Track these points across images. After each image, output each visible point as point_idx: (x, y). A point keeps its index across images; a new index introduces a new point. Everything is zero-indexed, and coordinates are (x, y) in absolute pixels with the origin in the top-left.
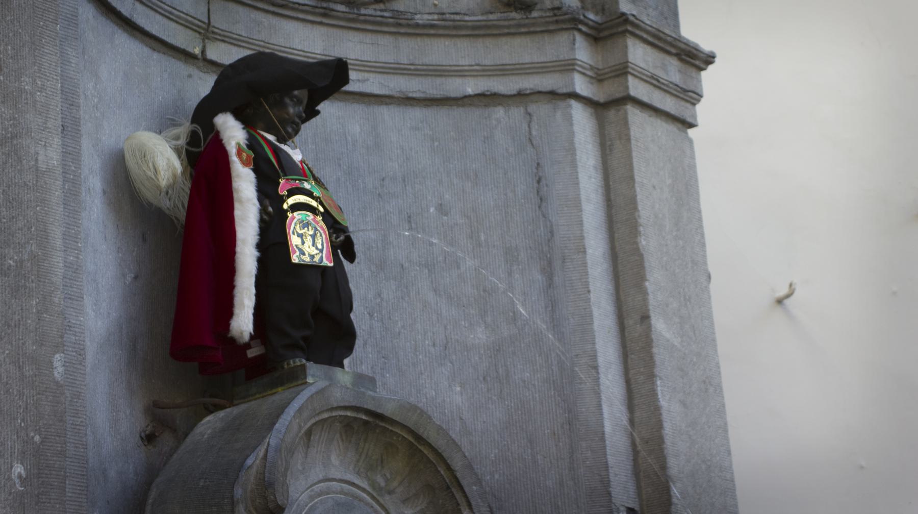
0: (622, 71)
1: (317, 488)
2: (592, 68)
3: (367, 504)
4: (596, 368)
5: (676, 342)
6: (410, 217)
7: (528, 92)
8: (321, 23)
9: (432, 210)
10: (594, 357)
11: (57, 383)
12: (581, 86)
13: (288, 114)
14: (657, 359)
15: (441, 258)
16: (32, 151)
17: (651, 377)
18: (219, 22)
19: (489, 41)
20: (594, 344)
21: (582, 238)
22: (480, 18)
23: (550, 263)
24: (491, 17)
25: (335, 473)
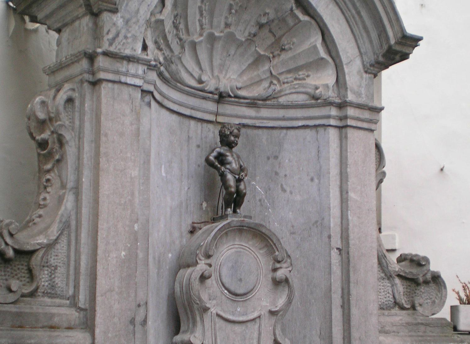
0: (346, 117)
1: (230, 247)
2: (337, 116)
3: (247, 250)
4: (330, 208)
5: (359, 199)
6: (280, 163)
7: (317, 124)
8: (254, 107)
9: (287, 161)
10: (330, 205)
11: (136, 231)
12: (332, 122)
13: (232, 140)
14: (349, 205)
15: (288, 175)
16: (130, 172)
17: (347, 210)
18: (221, 111)
19: (306, 110)
20: (330, 201)
21: (329, 169)
22: (303, 102)
23: (320, 176)
24: (306, 102)
25: (236, 243)
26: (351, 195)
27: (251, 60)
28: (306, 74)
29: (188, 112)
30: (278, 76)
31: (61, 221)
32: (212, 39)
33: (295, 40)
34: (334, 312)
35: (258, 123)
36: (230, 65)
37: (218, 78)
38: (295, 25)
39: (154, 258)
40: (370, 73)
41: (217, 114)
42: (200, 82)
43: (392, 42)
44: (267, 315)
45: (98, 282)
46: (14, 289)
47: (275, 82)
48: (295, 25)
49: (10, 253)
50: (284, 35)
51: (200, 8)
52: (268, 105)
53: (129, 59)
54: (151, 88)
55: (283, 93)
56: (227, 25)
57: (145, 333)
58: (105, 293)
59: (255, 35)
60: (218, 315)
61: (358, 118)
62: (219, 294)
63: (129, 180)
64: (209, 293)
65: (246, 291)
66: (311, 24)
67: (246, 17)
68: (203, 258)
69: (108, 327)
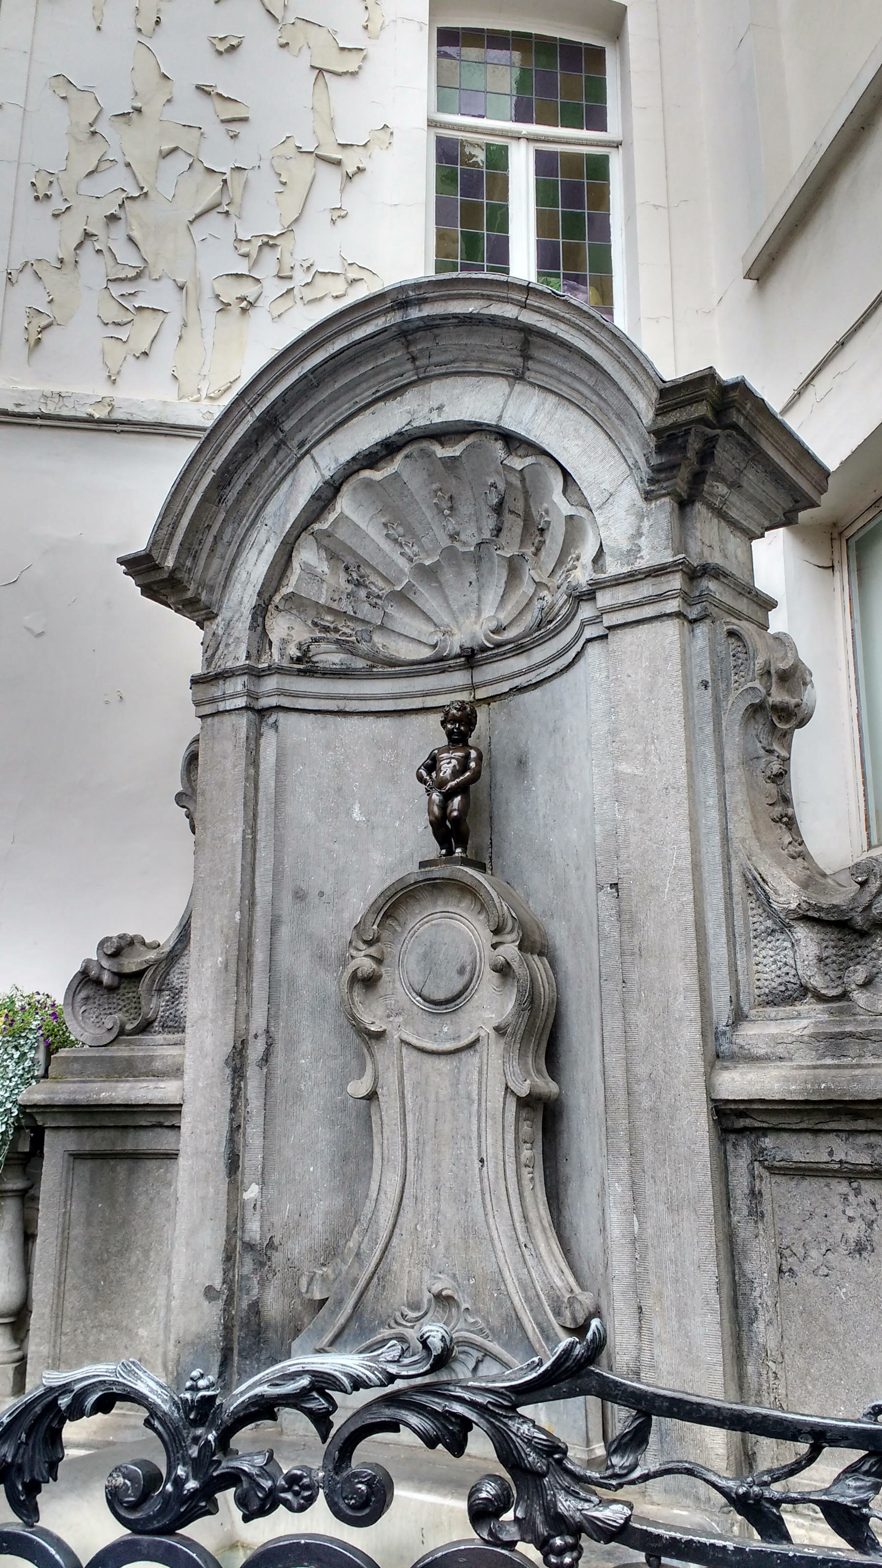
1: (425, 920)
8: (524, 651)
18: (478, 679)
27: (505, 574)
28: (574, 556)
29: (417, 703)
30: (545, 580)
32: (429, 574)
33: (545, 505)
34: (608, 1018)
35: (533, 677)
36: (479, 598)
38: (523, 480)
39: (320, 957)
42: (435, 646)
44: (493, 1034)
47: (546, 592)
48: (523, 480)
50: (527, 506)
51: (387, 536)
52: (537, 640)
54: (273, 701)
55: (557, 608)
56: (454, 537)
58: (196, 1022)
59: (498, 531)
60: (402, 1041)
61: (623, 604)
62: (408, 1005)
63: (229, 849)
64: (386, 1005)
65: (449, 995)
66: (540, 464)
67: (466, 509)
68: (364, 947)
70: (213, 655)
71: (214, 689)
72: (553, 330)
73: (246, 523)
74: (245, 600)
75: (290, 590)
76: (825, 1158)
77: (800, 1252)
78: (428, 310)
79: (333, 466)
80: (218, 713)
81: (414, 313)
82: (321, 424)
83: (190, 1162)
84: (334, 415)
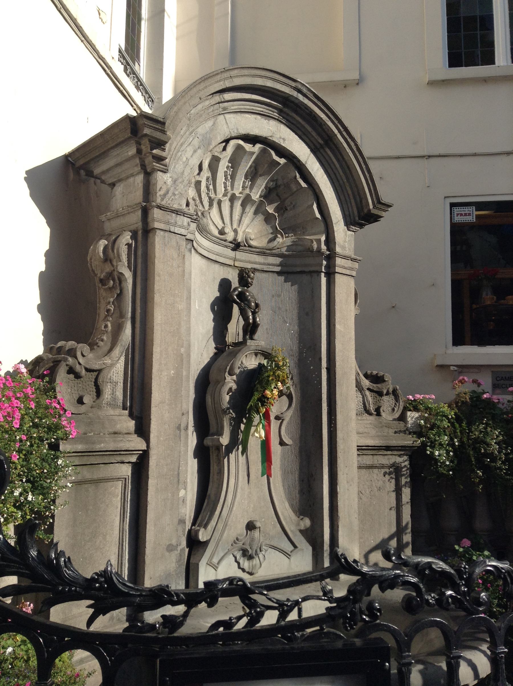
5: (342, 330)
26: (338, 327)
29: (213, 257)
31: (121, 345)
32: (233, 199)
37: (236, 231)
40: (351, 231)
41: (235, 260)
43: (371, 207)
45: (152, 395)
46: (85, 400)
47: (279, 236)
48: (297, 190)
49: (83, 372)
50: (287, 198)
51: (226, 172)
53: (177, 212)
57: (187, 435)
69: (160, 432)
70: (165, 195)
71: (169, 217)
72: (348, 151)
73: (191, 129)
74: (186, 174)
75: (200, 179)
76: (376, 462)
77: (363, 492)
78: (306, 101)
79: (236, 131)
80: (170, 232)
81: (301, 97)
82: (235, 106)
83: (156, 481)
84: (242, 107)
